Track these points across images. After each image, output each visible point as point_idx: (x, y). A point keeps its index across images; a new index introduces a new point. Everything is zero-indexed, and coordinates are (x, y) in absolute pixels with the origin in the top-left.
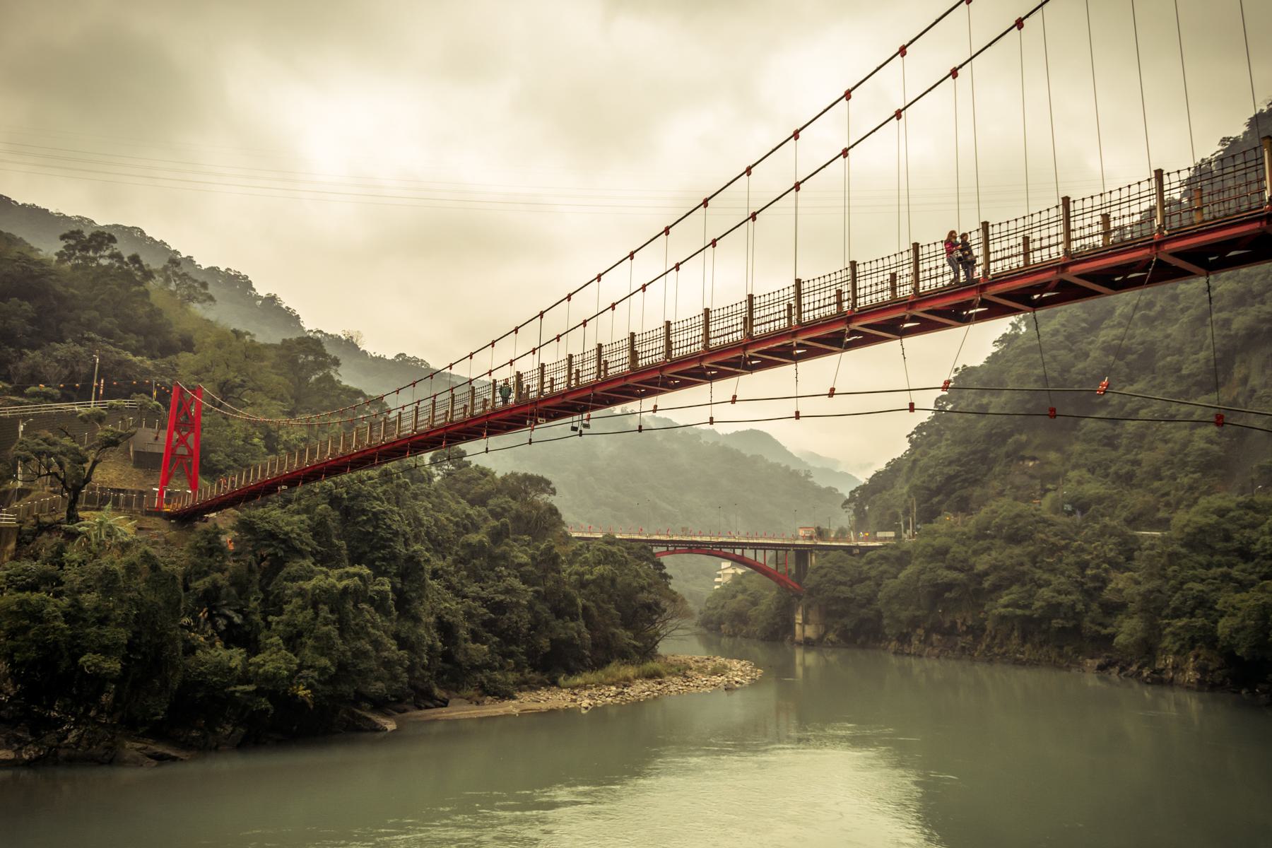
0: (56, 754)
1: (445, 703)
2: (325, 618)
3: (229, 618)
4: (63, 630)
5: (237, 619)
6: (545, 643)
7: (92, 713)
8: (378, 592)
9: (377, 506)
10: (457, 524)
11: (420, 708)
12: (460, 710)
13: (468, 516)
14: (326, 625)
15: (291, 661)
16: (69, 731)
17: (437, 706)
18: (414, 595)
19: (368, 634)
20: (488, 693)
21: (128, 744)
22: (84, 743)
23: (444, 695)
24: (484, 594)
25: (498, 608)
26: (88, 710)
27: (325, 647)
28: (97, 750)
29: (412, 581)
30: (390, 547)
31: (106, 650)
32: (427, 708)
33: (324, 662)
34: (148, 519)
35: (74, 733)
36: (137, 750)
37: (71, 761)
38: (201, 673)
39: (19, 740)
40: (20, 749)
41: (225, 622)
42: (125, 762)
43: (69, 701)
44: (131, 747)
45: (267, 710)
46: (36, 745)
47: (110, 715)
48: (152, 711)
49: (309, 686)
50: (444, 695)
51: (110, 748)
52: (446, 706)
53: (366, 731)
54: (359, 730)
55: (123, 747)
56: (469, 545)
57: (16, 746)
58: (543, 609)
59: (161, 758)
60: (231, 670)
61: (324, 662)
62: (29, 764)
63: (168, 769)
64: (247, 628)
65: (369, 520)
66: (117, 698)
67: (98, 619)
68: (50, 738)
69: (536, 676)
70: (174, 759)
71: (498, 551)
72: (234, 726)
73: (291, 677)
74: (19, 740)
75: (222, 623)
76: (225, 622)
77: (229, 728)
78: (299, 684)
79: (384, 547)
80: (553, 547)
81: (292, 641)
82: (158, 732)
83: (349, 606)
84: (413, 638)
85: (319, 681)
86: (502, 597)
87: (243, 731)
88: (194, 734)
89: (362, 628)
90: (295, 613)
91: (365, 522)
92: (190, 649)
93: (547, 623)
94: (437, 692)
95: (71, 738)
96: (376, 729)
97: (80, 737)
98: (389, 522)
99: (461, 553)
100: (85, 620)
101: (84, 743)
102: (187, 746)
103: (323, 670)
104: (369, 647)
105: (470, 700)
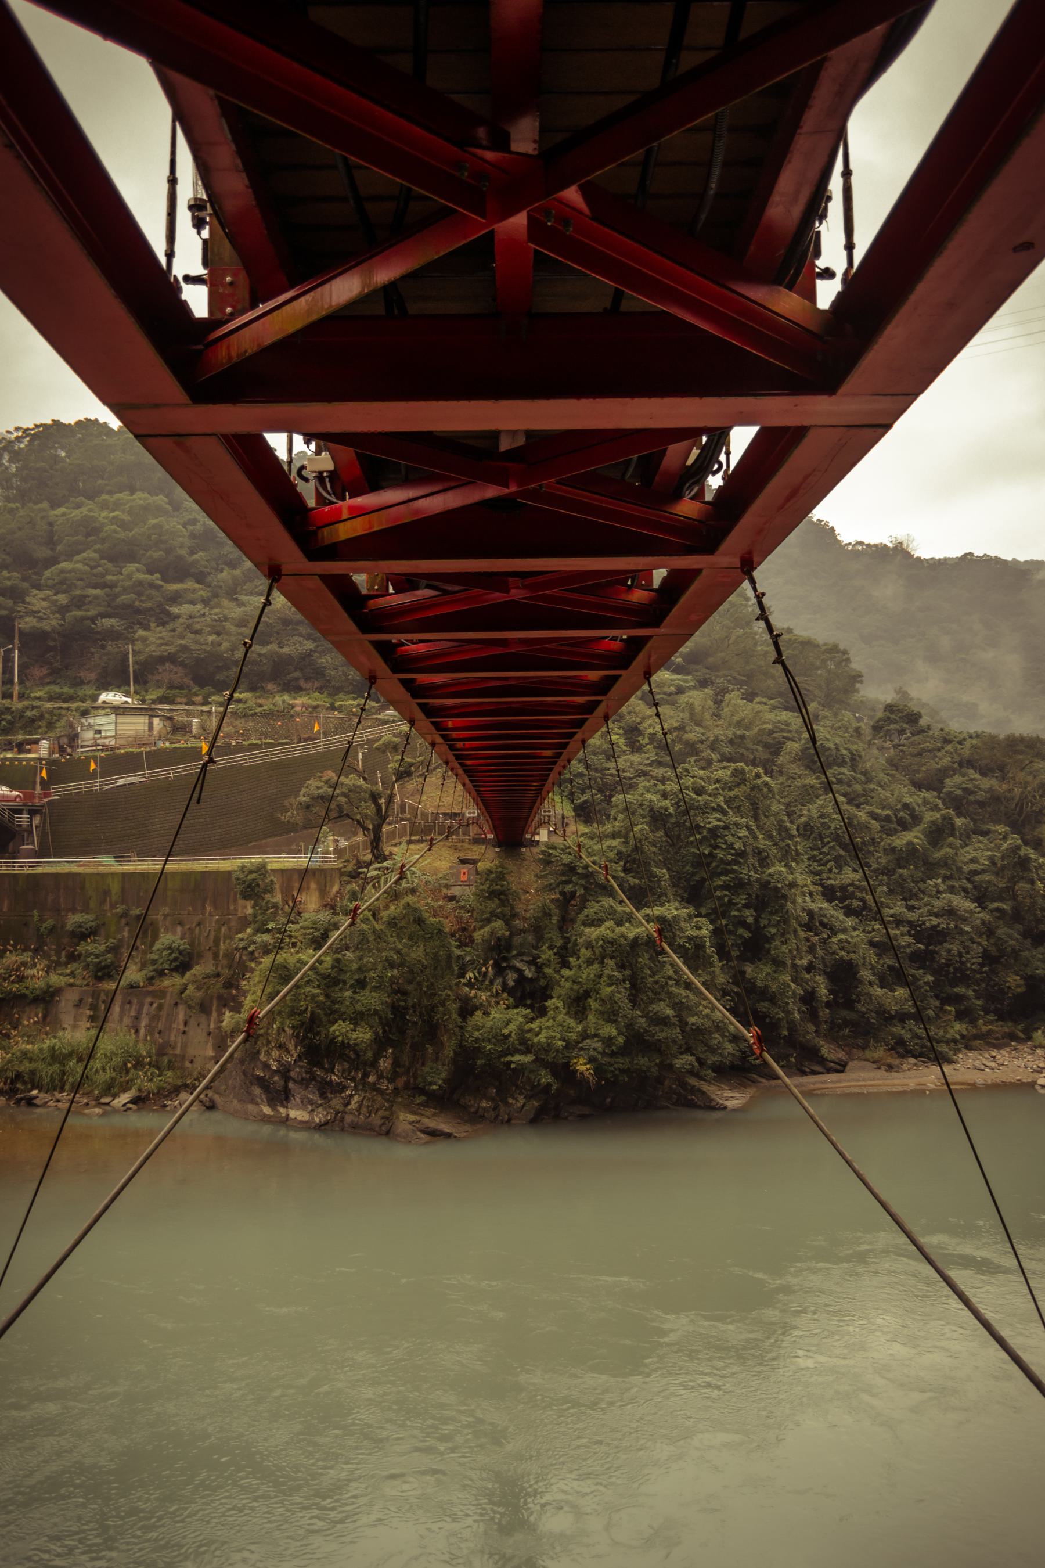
0: (342, 1120)
1: (841, 1068)
2: (610, 977)
3: (520, 972)
4: (314, 996)
5: (529, 973)
6: (1014, 981)
7: (371, 1079)
8: (690, 939)
9: (713, 820)
10: (887, 819)
11: (804, 1073)
12: (863, 1077)
13: (906, 806)
14: (609, 985)
15: (569, 1029)
16: (351, 1096)
17: (829, 1071)
18: (773, 931)
19: (670, 995)
20: (909, 1053)
21: (402, 1116)
22: (364, 1110)
23: (841, 1055)
24: (912, 916)
25: (934, 936)
26: (366, 1075)
27: (610, 1015)
28: (376, 1120)
29: (772, 913)
30: (734, 871)
31: (357, 1018)
32: (814, 1073)
33: (610, 1030)
34: (475, 848)
35: (356, 1098)
36: (411, 1123)
37: (355, 1129)
38: (477, 1040)
39: (311, 1102)
40: (313, 1110)
41: (515, 976)
42: (398, 1135)
43: (346, 1065)
44: (405, 1119)
45: (549, 1085)
46: (325, 1109)
47: (391, 1080)
48: (429, 1079)
49: (591, 1060)
50: (841, 1055)
51: (387, 1118)
52: (842, 1072)
53: (700, 1107)
54: (691, 1105)
55: (398, 1117)
56: (893, 849)
57: (310, 1108)
58: (1009, 935)
59: (434, 1134)
60: (507, 1037)
61: (610, 1030)
62: (321, 1127)
63: (441, 1151)
64: (543, 982)
65: (704, 838)
66: (396, 1063)
67: (357, 981)
68: (336, 1102)
69: (1000, 1028)
70: (448, 1136)
71: (938, 855)
72: (528, 1098)
73: (569, 1045)
74: (311, 1102)
75: (511, 978)
76: (515, 976)
77: (522, 1100)
78: (578, 1057)
79: (726, 872)
80: (1018, 848)
81: (578, 1004)
82: (445, 1101)
83: (644, 959)
84: (774, 987)
85: (604, 1054)
86: (935, 921)
87: (536, 1104)
88: (484, 1104)
89: (662, 987)
90: (580, 972)
91: (701, 842)
92: (467, 1009)
93: (1016, 954)
94: (828, 1051)
95: (353, 1105)
96: (711, 1106)
97: (360, 1104)
98: (730, 839)
99: (883, 861)
100: (345, 982)
101: (364, 1110)
102: (475, 1118)
103: (609, 1041)
104: (670, 1012)
105: (877, 1063)
